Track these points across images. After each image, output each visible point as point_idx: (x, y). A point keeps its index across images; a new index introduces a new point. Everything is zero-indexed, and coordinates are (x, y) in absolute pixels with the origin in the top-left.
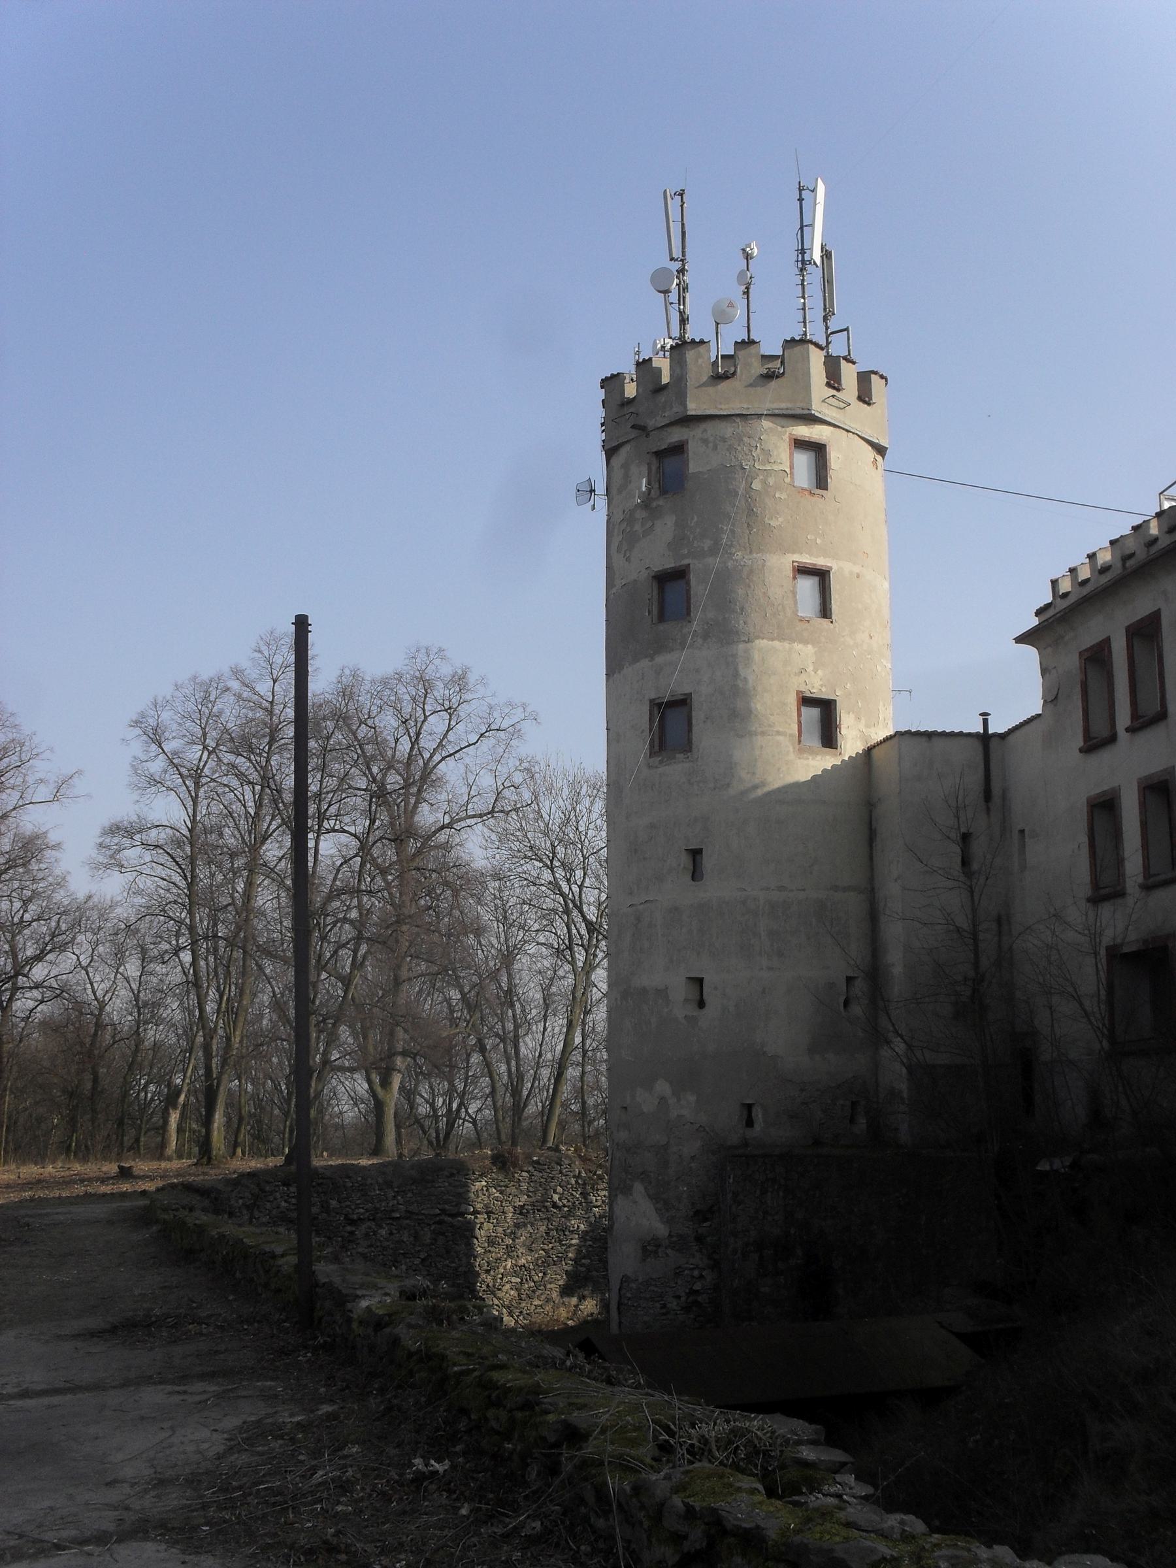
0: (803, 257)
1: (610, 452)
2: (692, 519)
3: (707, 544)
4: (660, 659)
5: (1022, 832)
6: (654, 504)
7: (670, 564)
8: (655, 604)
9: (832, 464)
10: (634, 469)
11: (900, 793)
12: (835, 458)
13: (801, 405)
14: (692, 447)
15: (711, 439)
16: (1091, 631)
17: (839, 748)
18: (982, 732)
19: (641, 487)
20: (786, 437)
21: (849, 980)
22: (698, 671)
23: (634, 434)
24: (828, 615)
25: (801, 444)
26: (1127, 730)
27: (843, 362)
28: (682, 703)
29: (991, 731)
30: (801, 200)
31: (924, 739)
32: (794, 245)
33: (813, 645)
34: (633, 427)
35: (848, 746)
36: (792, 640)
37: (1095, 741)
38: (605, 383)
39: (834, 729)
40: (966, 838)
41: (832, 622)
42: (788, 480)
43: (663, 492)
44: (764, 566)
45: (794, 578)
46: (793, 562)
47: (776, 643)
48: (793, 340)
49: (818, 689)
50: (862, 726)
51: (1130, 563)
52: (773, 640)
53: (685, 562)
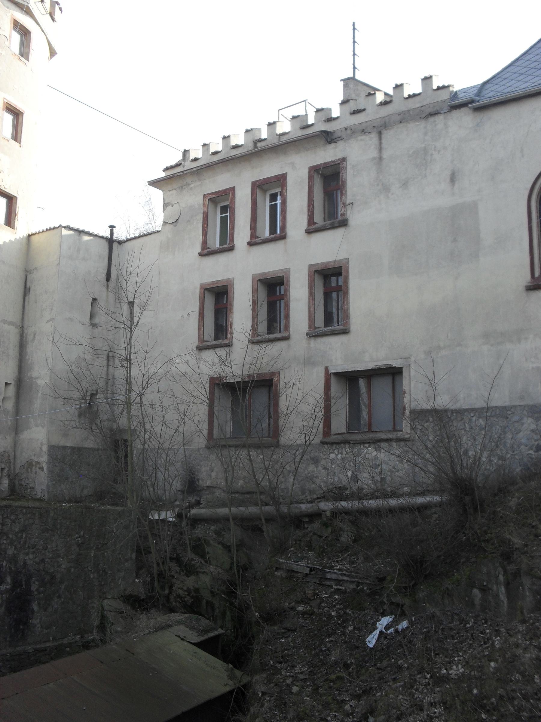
17: (15, 229)
18: (109, 237)
21: (6, 384)
24: (18, 139)
25: (19, 27)
29: (114, 238)
31: (77, 233)
37: (208, 250)
40: (94, 300)
41: (20, 146)
46: (4, 98)
51: (259, 145)
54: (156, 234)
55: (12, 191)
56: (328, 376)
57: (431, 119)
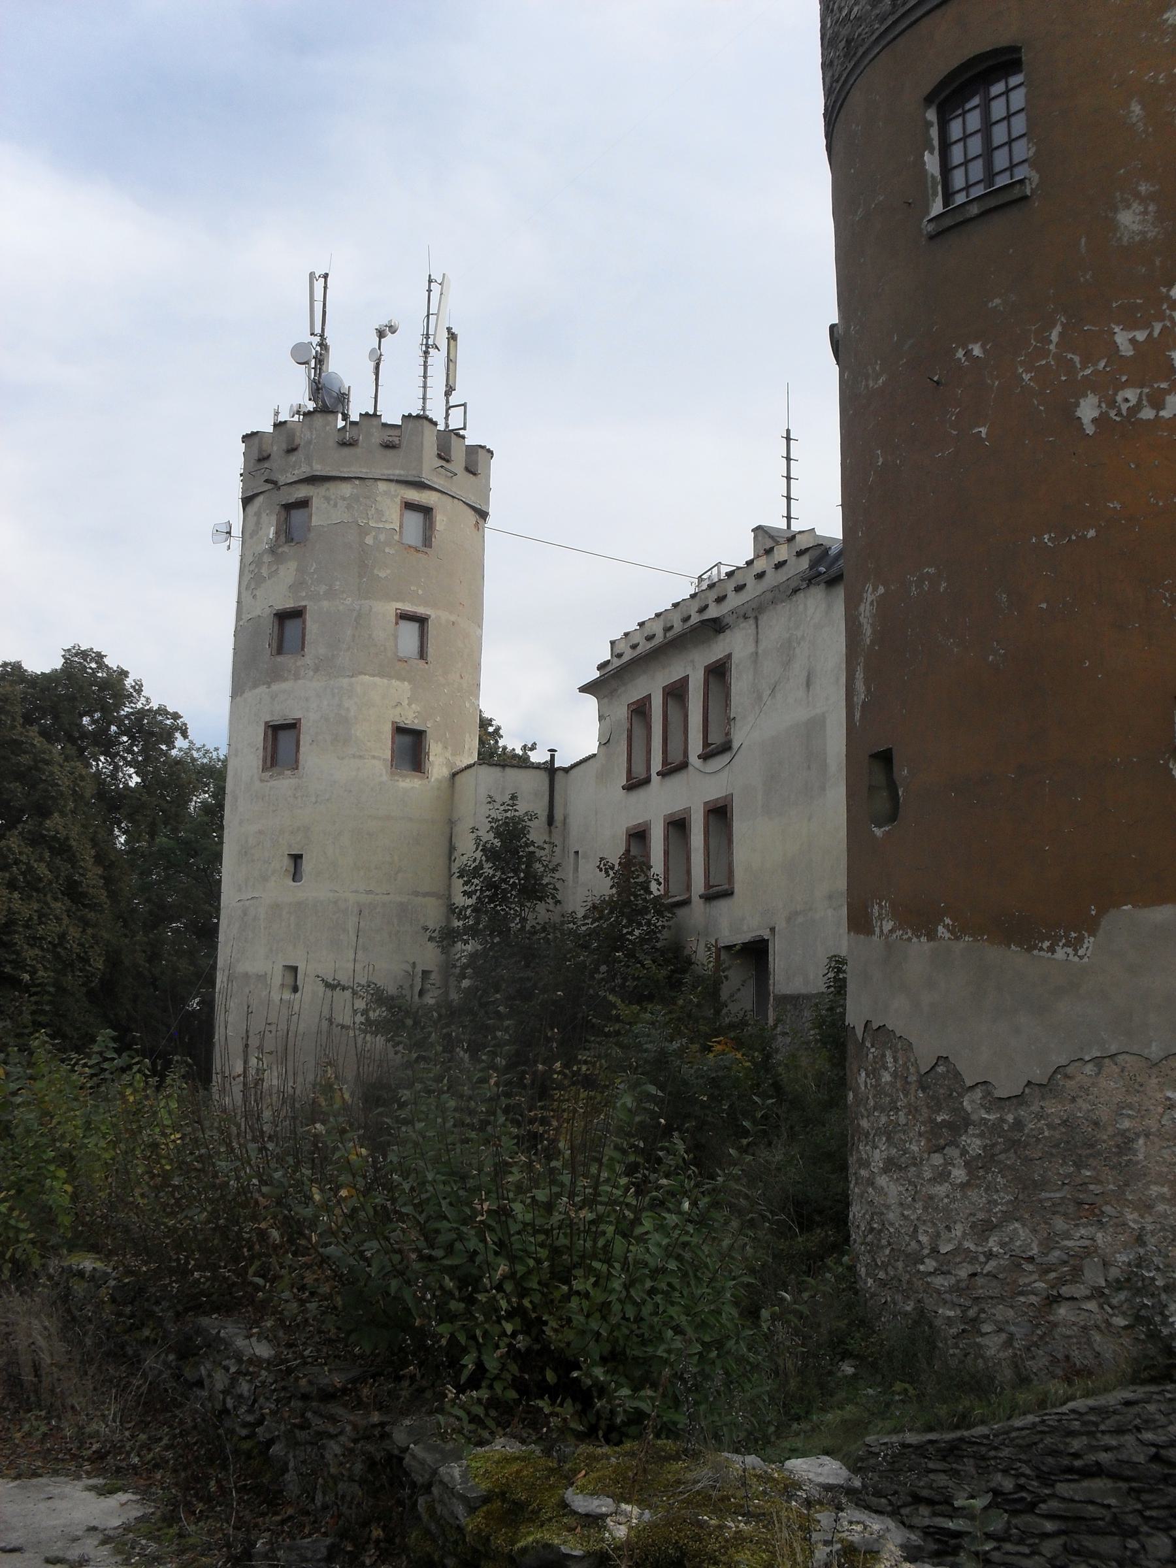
0: (427, 341)
1: (247, 501)
2: (312, 565)
3: (323, 589)
4: (275, 687)
5: (577, 853)
6: (280, 550)
7: (289, 604)
8: (275, 637)
9: (438, 524)
10: (264, 515)
11: (475, 814)
12: (440, 520)
13: (414, 472)
14: (315, 503)
15: (333, 497)
16: (635, 692)
19: (269, 534)
20: (398, 500)
22: (307, 699)
23: (270, 486)
25: (409, 506)
26: (658, 774)
27: (453, 436)
28: (293, 726)
30: (429, 291)
32: (421, 330)
33: (409, 682)
34: (266, 481)
35: (435, 771)
36: (390, 677)
38: (246, 438)
39: (423, 756)
42: (397, 537)
43: (289, 539)
44: (370, 610)
45: (397, 623)
47: (377, 679)
48: (410, 415)
49: (410, 719)
50: (448, 754)
52: (374, 676)
53: (303, 603)
54: (594, 759)
55: (417, 725)
56: (719, 950)
57: (794, 598)
